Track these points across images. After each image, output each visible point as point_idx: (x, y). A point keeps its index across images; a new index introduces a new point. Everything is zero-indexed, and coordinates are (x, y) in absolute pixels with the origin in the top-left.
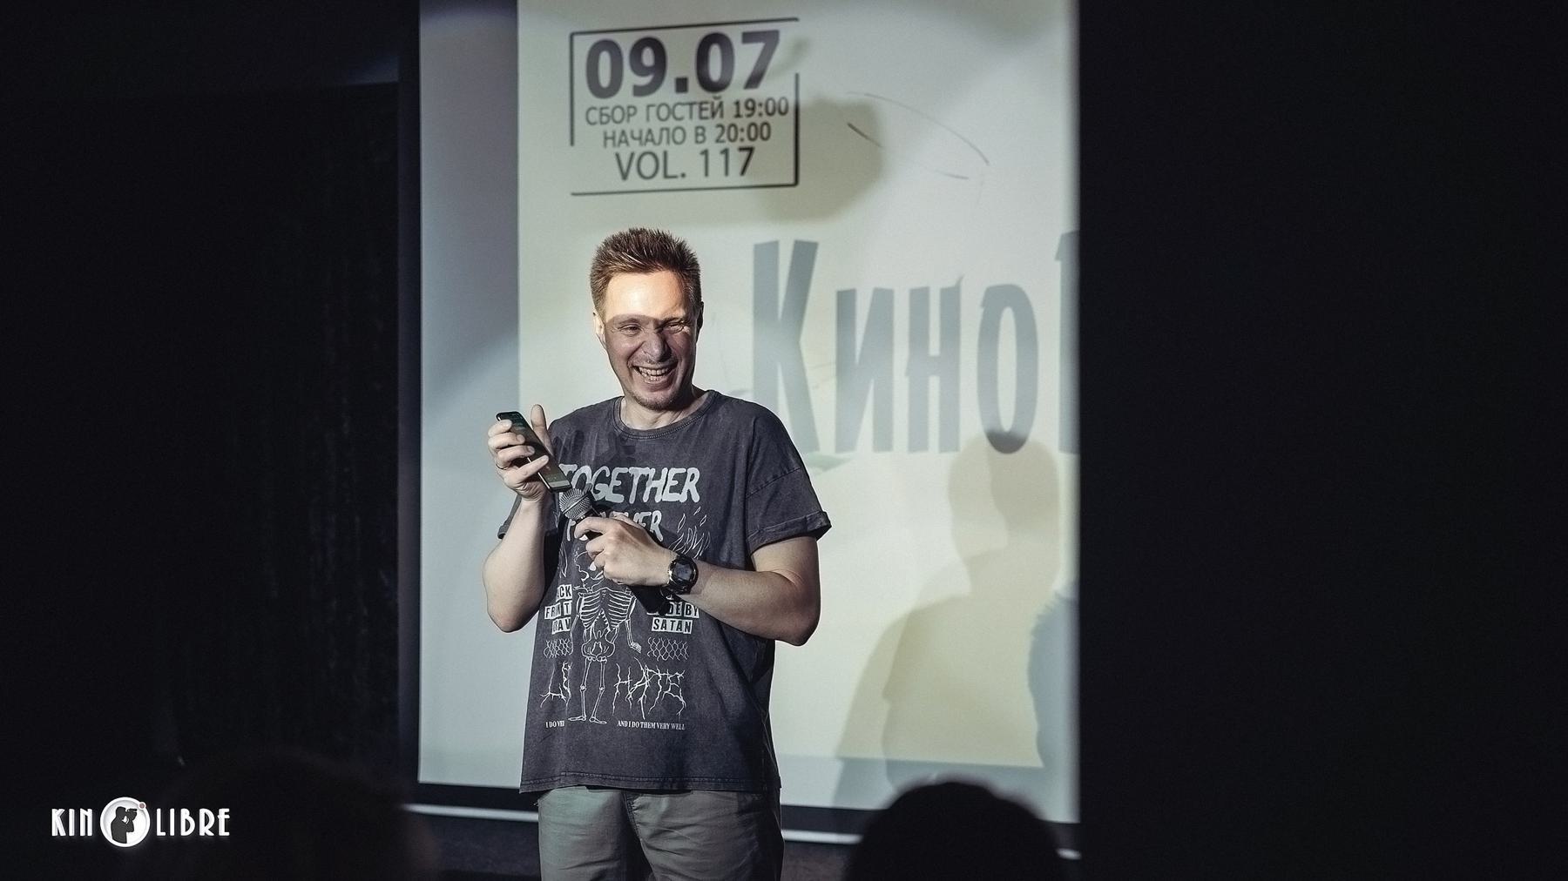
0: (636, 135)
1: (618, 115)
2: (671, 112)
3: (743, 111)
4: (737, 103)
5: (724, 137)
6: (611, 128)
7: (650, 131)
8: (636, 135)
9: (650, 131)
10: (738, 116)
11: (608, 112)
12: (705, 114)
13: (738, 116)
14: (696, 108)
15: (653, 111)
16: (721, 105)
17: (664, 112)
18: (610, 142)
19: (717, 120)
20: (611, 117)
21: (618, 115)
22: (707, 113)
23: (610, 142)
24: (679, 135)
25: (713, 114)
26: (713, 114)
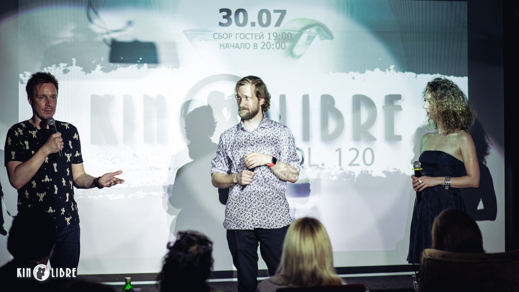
0: (232, 45)
1: (225, 36)
2: (245, 36)
3: (272, 38)
4: (269, 34)
5: (265, 47)
6: (223, 41)
7: (237, 44)
8: (232, 45)
9: (237, 44)
10: (270, 39)
11: (222, 35)
12: (257, 38)
13: (270, 39)
14: (254, 36)
15: (238, 36)
16: (263, 35)
17: (242, 36)
18: (222, 47)
19: (262, 40)
20: (223, 37)
21: (225, 36)
22: (258, 38)
23: (222, 47)
24: (248, 46)
25: (260, 38)
26: (260, 38)
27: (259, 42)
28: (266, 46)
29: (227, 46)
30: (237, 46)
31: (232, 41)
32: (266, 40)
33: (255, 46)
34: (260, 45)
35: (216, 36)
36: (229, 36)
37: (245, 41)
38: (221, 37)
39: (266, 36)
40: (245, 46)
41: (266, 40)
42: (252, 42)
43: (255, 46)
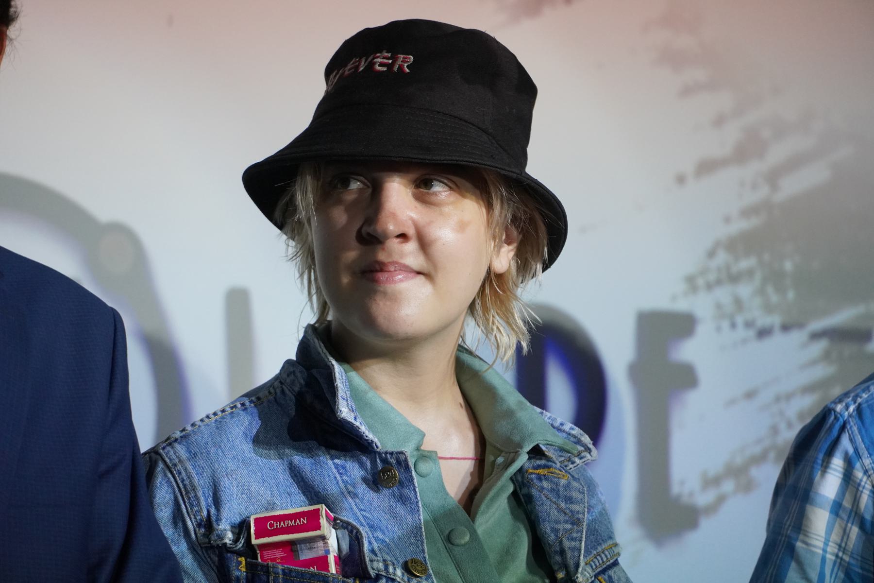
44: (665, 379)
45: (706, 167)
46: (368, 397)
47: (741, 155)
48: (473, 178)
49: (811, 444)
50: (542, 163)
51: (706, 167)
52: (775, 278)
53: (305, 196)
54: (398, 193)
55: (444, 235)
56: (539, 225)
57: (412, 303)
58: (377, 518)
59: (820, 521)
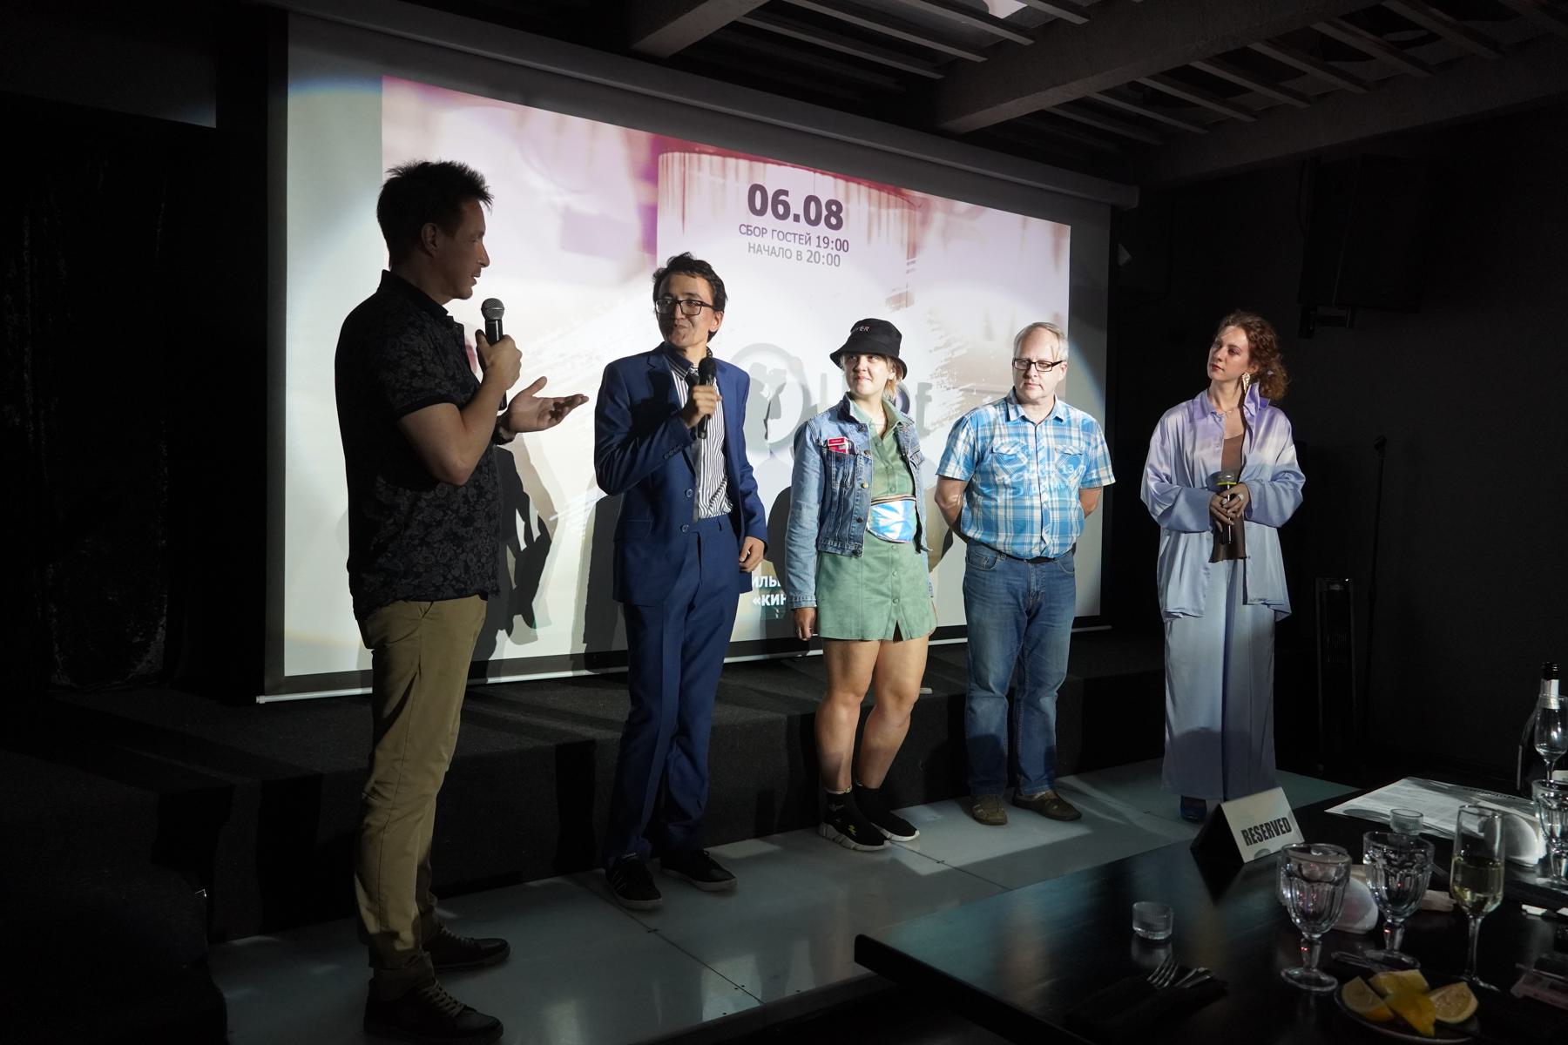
6: (753, 240)
19: (808, 247)
27: (804, 248)
28: (814, 258)
29: (759, 250)
30: (772, 252)
31: (766, 241)
32: (814, 249)
33: (799, 254)
34: (806, 255)
35: (744, 229)
36: (763, 231)
37: (784, 244)
38: (748, 230)
39: (814, 241)
40: (784, 253)
41: (814, 249)
42: (795, 246)
43: (799, 254)
44: (924, 399)
45: (937, 349)
46: (855, 409)
47: (946, 346)
48: (883, 356)
49: (959, 425)
50: (902, 355)
51: (937, 349)
52: (952, 376)
53: (843, 361)
54: (864, 359)
55: (876, 371)
56: (901, 369)
57: (866, 386)
58: (855, 437)
59: (960, 444)
